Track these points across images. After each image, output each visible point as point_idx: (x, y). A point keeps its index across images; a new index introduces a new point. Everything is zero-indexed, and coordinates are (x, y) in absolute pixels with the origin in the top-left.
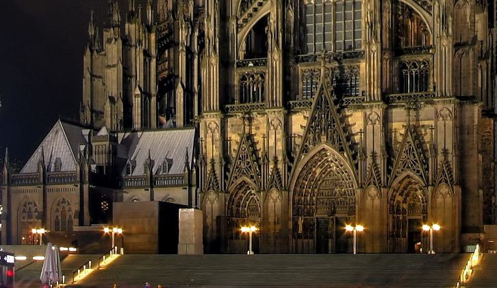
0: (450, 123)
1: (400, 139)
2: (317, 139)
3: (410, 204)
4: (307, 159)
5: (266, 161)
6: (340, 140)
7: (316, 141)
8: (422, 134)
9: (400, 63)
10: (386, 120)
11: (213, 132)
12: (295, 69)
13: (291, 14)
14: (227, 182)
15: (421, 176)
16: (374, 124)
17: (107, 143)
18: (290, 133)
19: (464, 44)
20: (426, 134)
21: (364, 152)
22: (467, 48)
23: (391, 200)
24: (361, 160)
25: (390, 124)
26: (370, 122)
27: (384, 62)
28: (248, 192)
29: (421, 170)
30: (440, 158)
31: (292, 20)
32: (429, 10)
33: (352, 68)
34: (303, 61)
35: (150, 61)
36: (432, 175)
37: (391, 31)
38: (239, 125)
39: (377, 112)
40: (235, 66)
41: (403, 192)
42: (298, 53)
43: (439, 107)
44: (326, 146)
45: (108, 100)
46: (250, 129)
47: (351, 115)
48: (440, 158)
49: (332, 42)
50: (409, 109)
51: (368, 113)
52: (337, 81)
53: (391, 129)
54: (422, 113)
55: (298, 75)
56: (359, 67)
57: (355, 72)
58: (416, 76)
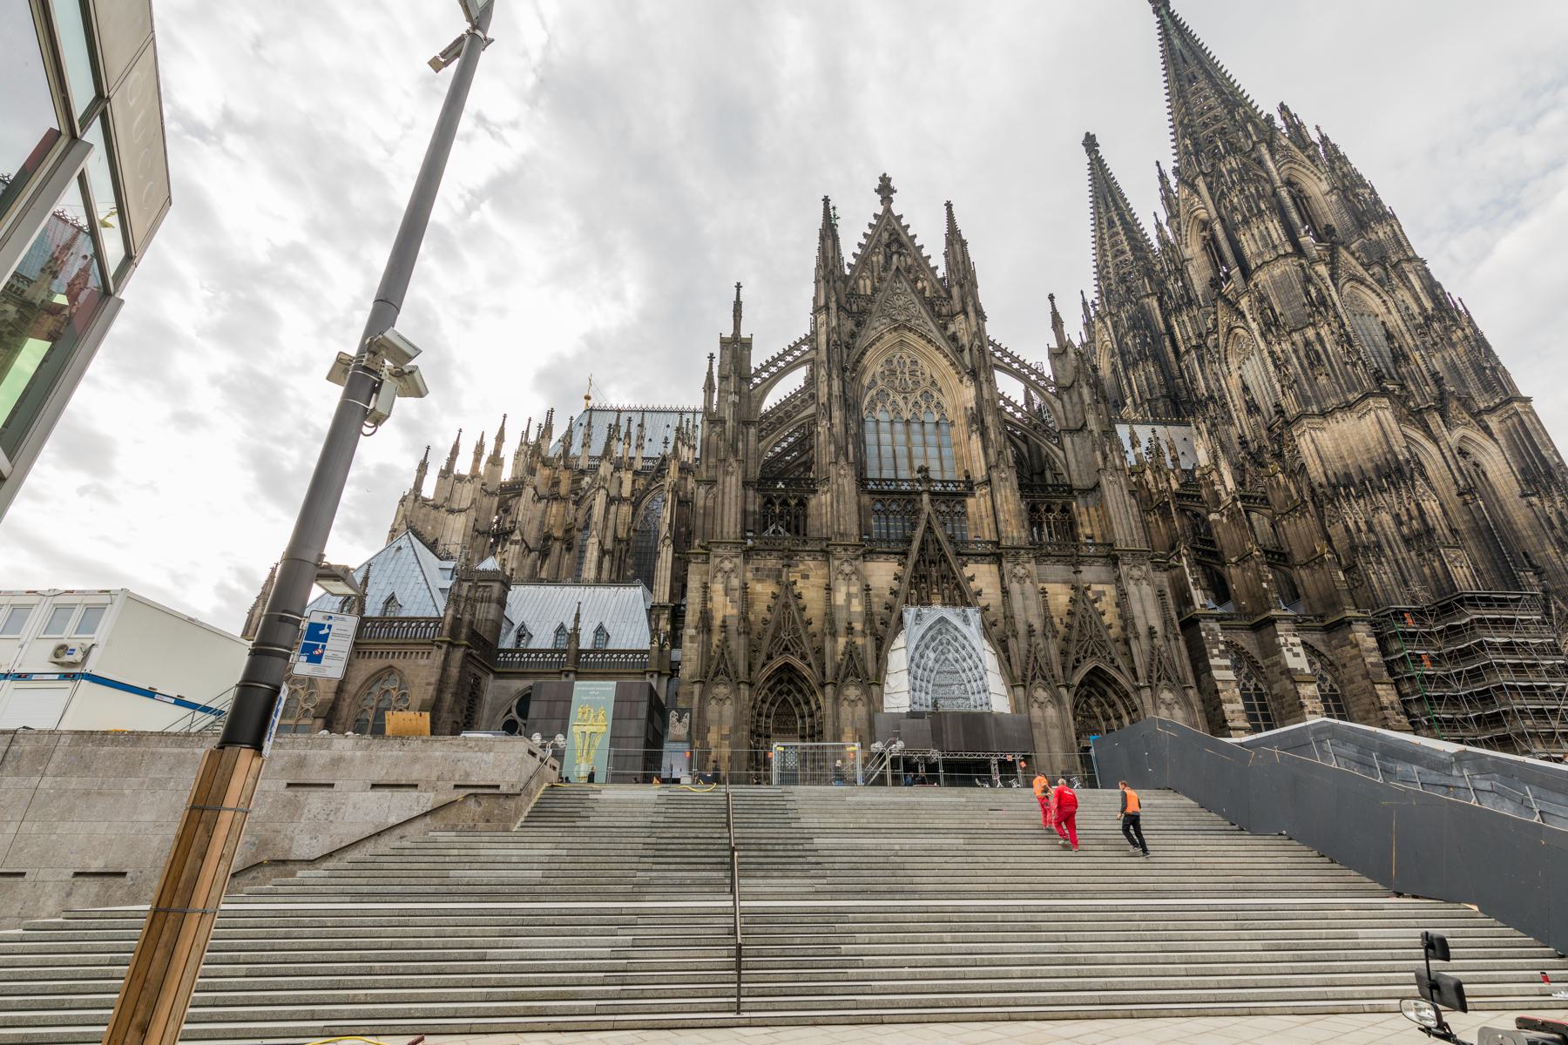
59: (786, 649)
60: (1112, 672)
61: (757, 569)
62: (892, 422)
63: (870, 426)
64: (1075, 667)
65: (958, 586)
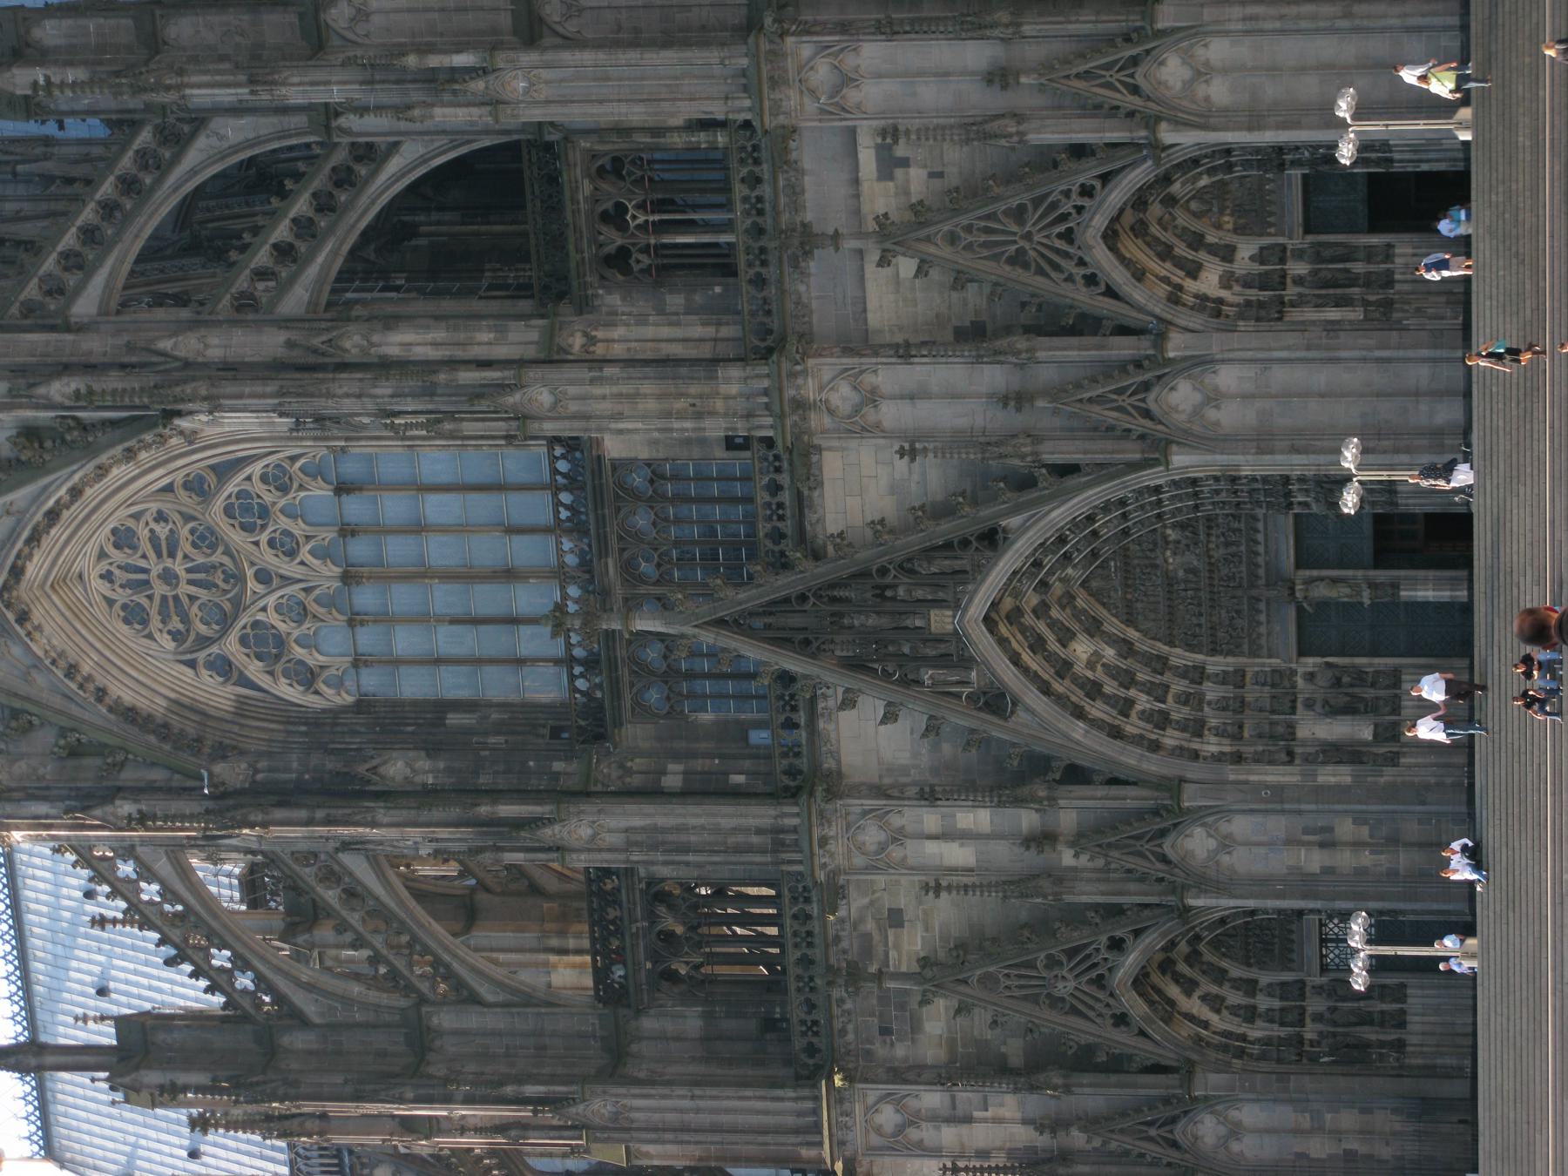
2: (942, 648)
3: (1238, 230)
4: (1032, 697)
6: (948, 546)
7: (955, 655)
15: (1105, 178)
32: (370, 154)
38: (884, 999)
41: (1180, 263)
44: (978, 607)
59: (1099, 982)
60: (1118, 195)
61: (885, 1031)
62: (355, 620)
63: (371, 681)
64: (1111, 293)
65: (906, 568)
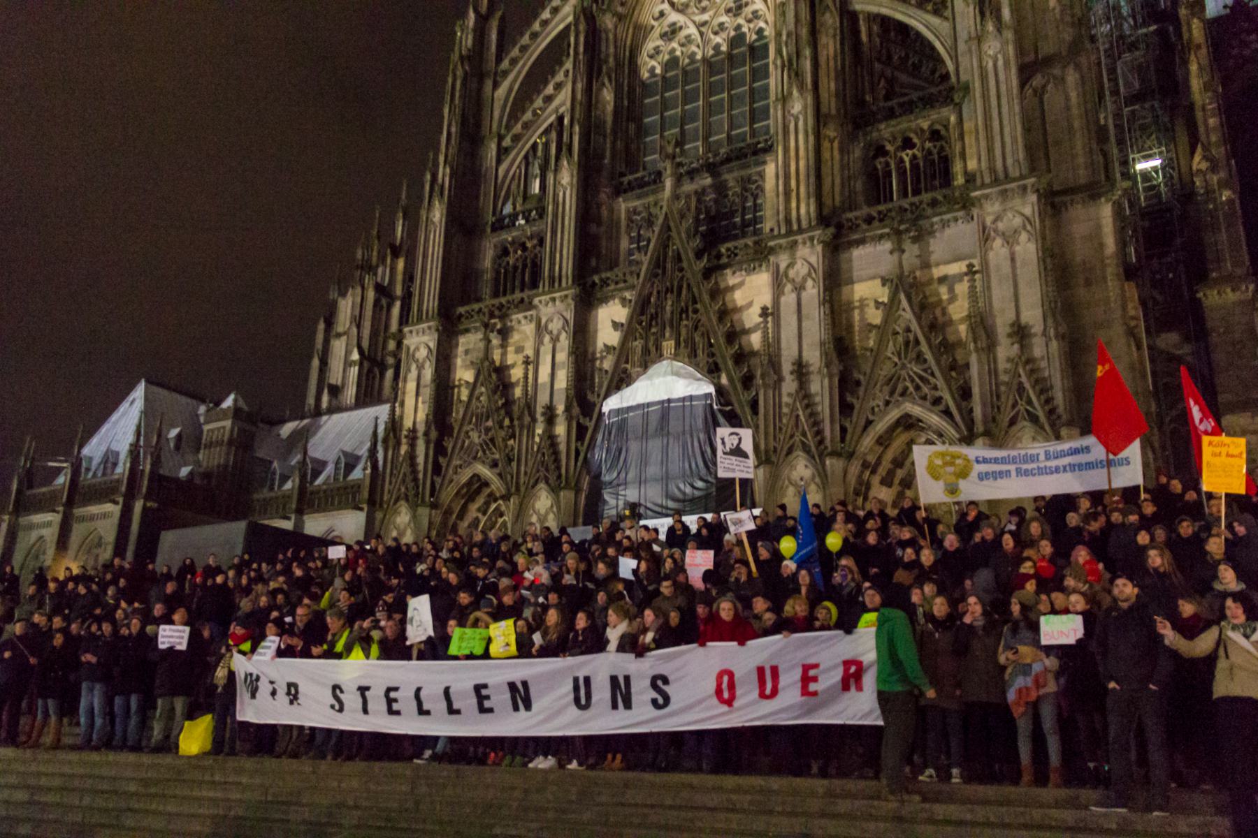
0: (1028, 248)
1: (875, 316)
2: (653, 349)
5: (527, 419)
8: (941, 300)
9: (867, 147)
10: (834, 280)
11: (420, 368)
12: (611, 211)
13: (608, 95)
14: (438, 480)
16: (799, 289)
17: (228, 423)
18: (591, 350)
19: (1048, 61)
20: (953, 298)
21: (774, 363)
22: (1057, 71)
23: (857, 493)
24: (766, 386)
25: (845, 290)
26: (789, 287)
27: (826, 144)
28: (493, 506)
29: (947, 397)
30: (1006, 350)
31: (610, 108)
33: (745, 182)
34: (631, 187)
35: (390, 307)
36: (984, 405)
37: (840, 74)
39: (807, 257)
40: (489, 230)
41: (891, 474)
42: (622, 175)
43: (992, 208)
45: (326, 391)
46: (504, 354)
47: (741, 284)
48: (1006, 350)
49: (700, 143)
50: (898, 233)
51: (783, 266)
52: (711, 219)
53: (850, 303)
54: (938, 246)
55: (619, 218)
56: (762, 175)
57: (751, 188)
58: (915, 166)
